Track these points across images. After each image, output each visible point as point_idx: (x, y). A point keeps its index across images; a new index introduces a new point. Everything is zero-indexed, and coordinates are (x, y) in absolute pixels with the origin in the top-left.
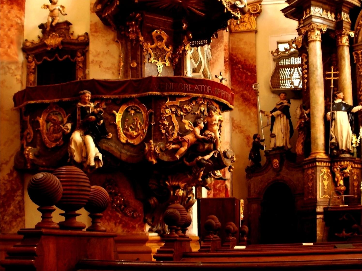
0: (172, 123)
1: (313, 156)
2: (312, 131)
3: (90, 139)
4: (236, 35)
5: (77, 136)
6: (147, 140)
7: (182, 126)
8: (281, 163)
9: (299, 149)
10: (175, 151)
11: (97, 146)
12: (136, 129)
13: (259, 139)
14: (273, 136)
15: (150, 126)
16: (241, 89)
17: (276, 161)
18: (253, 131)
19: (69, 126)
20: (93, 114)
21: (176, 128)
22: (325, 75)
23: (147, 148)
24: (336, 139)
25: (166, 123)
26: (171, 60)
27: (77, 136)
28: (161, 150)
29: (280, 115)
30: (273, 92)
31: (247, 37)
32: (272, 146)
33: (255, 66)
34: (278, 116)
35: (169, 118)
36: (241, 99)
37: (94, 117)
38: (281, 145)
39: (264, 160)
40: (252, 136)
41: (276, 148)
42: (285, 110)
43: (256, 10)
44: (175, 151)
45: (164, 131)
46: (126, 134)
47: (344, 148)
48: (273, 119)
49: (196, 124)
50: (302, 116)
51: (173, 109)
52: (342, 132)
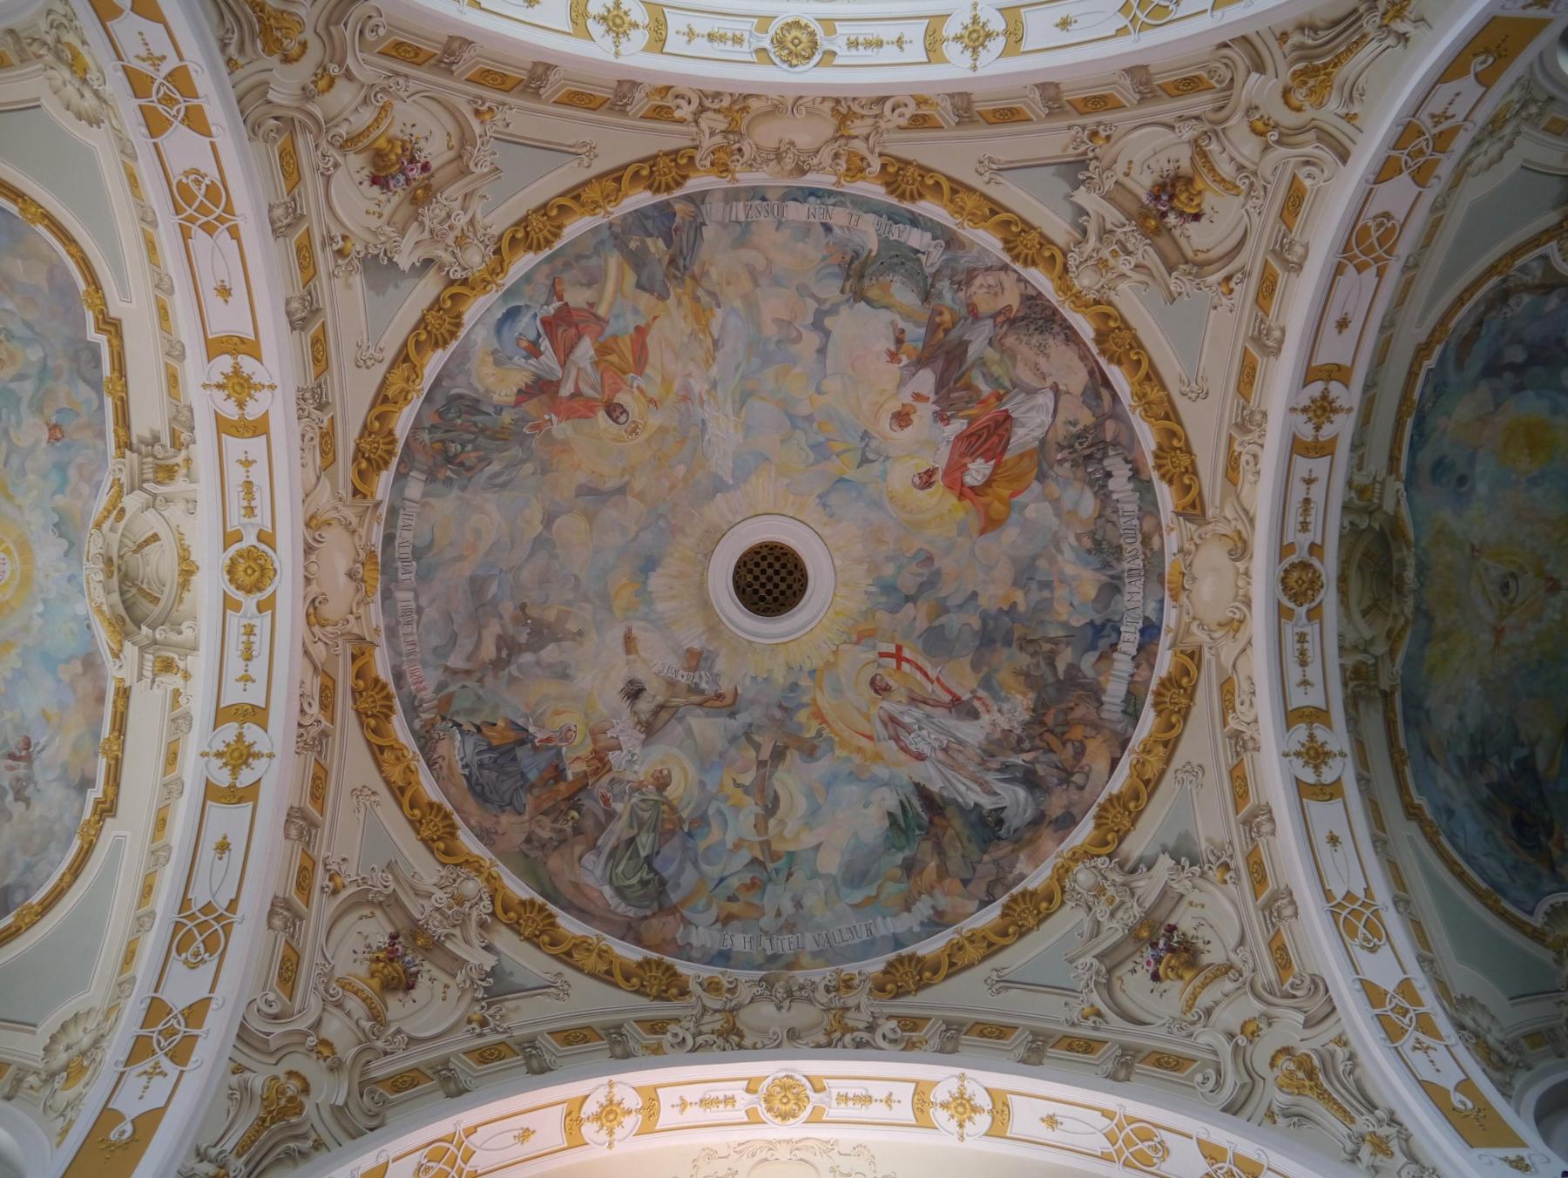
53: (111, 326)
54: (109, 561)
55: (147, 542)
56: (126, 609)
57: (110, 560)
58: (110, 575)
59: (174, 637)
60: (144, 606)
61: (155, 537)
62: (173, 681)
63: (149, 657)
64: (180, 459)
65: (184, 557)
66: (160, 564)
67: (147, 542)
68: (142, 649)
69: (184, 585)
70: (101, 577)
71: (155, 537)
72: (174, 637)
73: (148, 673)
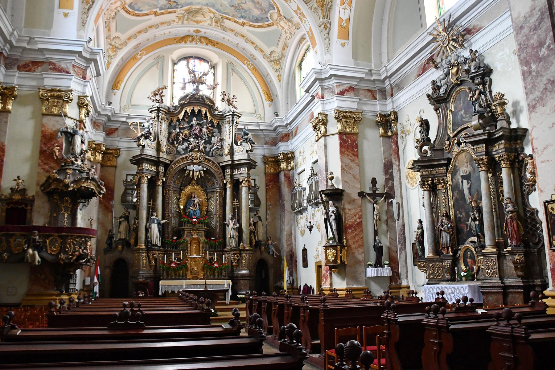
0: (70, 246)
1: (138, 247)
2: (139, 233)
3: (36, 253)
4: (105, 168)
5: (30, 251)
6: (59, 253)
7: (75, 248)
8: (123, 248)
9: (132, 241)
10: (71, 258)
11: (39, 256)
12: (55, 248)
13: (112, 233)
14: (120, 232)
15: (61, 247)
16: (104, 201)
17: (120, 246)
18: (109, 228)
19: (26, 245)
20: (38, 242)
21: (72, 248)
22: (148, 204)
23: (60, 257)
24: (151, 239)
25: (68, 246)
26: (71, 211)
27: (30, 251)
28: (65, 258)
29: (124, 221)
30: (122, 205)
31: (111, 170)
32: (118, 237)
33: (114, 188)
34: (123, 221)
35: (70, 244)
36: (104, 207)
37: (38, 243)
38: (124, 238)
39: (114, 245)
40: (109, 230)
41: (120, 239)
42: (127, 218)
43: (117, 154)
44: (71, 258)
45: (67, 249)
46: (50, 250)
47: (154, 244)
48: (120, 222)
49: (80, 248)
50: (135, 224)
51: (72, 240)
52: (154, 235)
53: (243, 24)
54: (201, 9)
55: (204, 15)
56: (191, 11)
57: (201, 9)
58: (198, 9)
59: (185, 19)
60: (192, 14)
61: (205, 17)
62: (177, 20)
63: (182, 15)
64: (218, 25)
65: (200, 22)
66: (199, 18)
67: (204, 15)
68: (183, 14)
69: (195, 21)
70: (198, 8)
71: (205, 17)
72: (185, 19)
73: (178, 15)
